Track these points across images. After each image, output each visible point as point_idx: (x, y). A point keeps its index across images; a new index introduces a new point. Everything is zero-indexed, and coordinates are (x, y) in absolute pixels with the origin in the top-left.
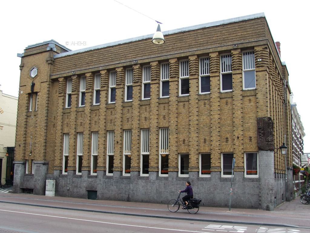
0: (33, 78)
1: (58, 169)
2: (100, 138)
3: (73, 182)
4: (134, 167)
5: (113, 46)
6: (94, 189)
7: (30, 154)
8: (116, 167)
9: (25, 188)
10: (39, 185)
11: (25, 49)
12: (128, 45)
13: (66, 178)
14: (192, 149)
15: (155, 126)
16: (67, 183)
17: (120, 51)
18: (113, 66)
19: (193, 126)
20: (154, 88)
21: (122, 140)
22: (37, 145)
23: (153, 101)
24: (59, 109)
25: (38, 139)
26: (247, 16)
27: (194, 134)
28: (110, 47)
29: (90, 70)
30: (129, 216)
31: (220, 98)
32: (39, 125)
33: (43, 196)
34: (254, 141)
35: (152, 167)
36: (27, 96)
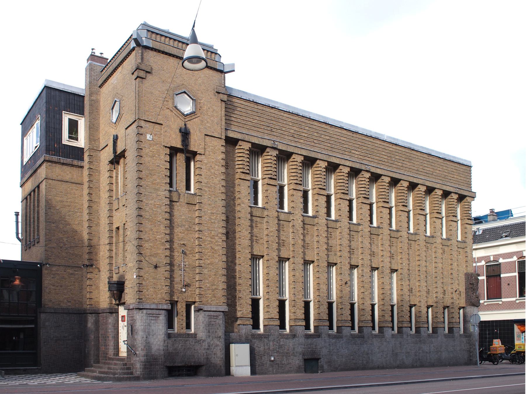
0: (183, 114)
1: (248, 322)
2: (320, 273)
3: (280, 347)
4: (367, 321)
5: (332, 126)
6: (316, 356)
7: (184, 290)
8: (345, 320)
9: (179, 365)
10: (218, 358)
11: (142, 23)
12: (351, 134)
13: (266, 340)
14: (422, 301)
15: (388, 267)
16: (269, 349)
17: (342, 138)
18: (338, 159)
19: (422, 272)
20: (385, 213)
21: (352, 280)
22: (205, 271)
23: (385, 232)
24: (242, 205)
25: (207, 259)
26: (425, 148)
27: (423, 282)
28: (328, 124)
29: (305, 153)
30: (327, 391)
31: (409, 240)
32: (208, 230)
33: (227, 379)
34: (463, 295)
35: (386, 321)
36: (168, 151)
